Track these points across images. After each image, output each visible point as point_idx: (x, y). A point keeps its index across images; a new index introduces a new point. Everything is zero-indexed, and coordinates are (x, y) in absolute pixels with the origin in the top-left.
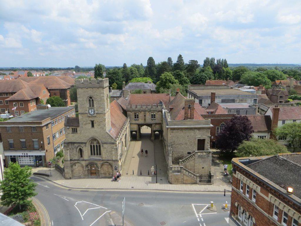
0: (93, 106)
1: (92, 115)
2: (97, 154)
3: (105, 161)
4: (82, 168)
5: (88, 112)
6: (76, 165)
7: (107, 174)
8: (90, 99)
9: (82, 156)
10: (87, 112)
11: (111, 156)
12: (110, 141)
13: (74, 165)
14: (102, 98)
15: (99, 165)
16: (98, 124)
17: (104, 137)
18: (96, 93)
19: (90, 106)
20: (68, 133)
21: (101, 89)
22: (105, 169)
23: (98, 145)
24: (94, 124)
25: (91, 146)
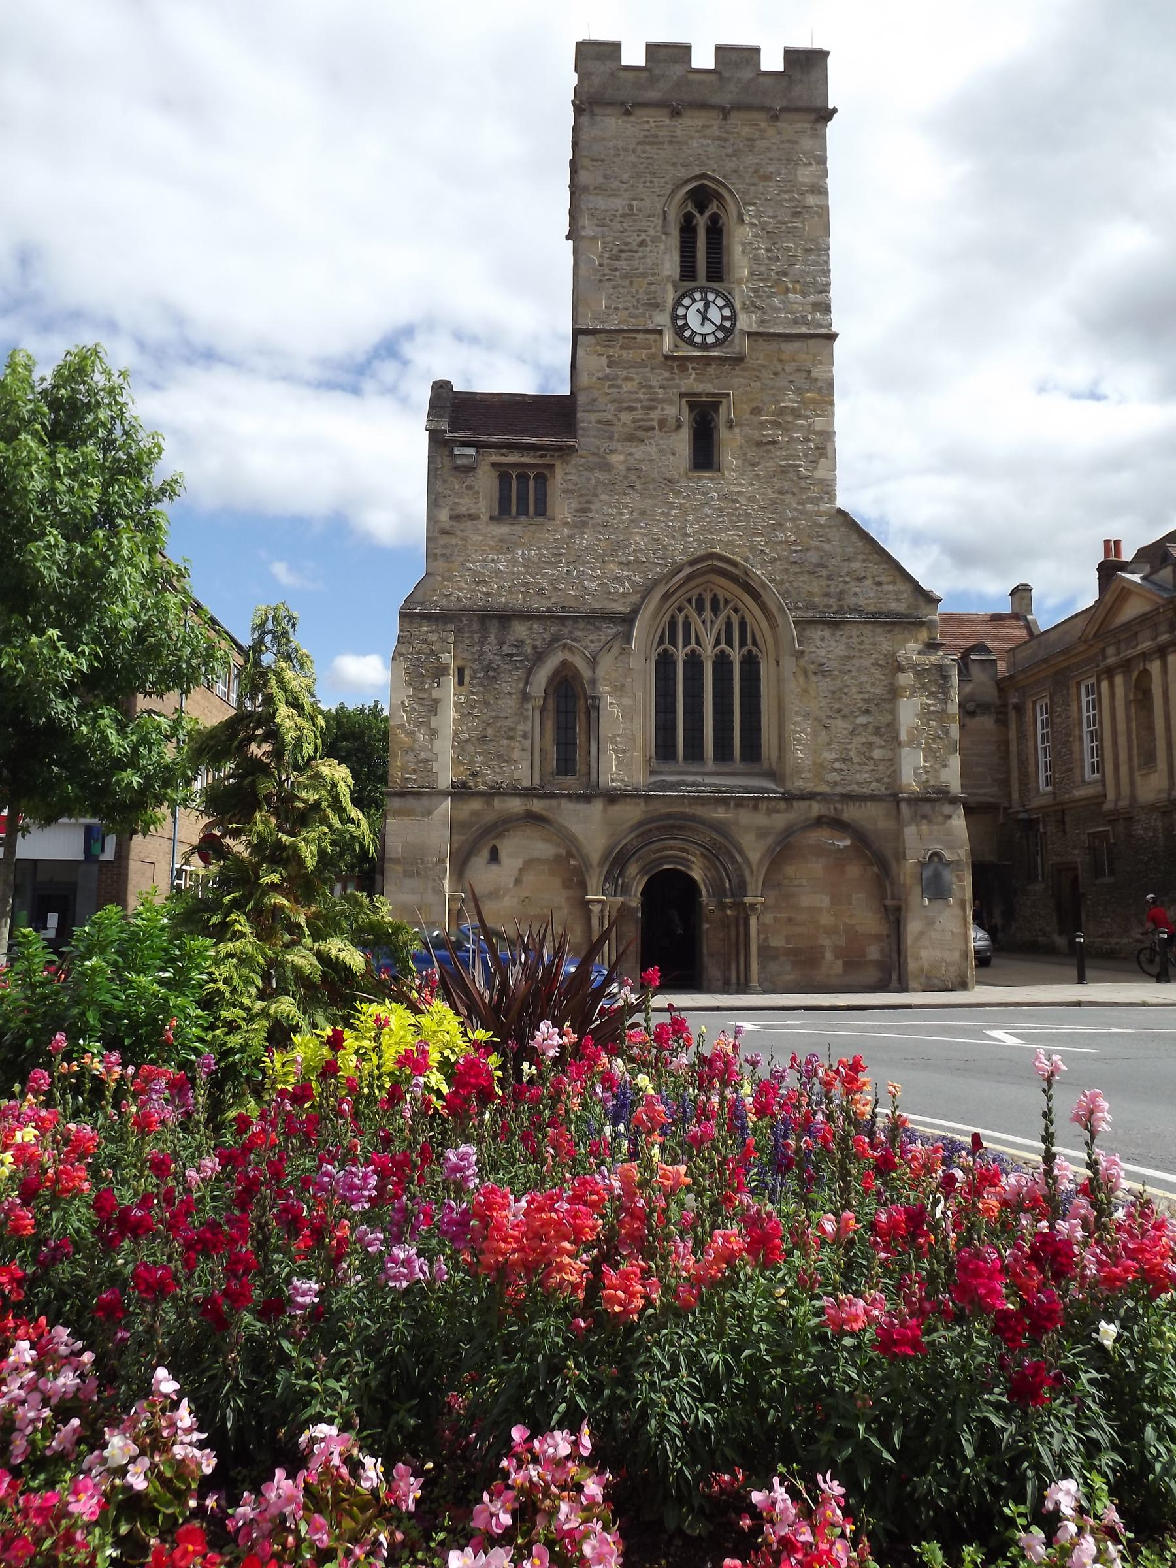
0: (717, 271)
1: (704, 346)
2: (723, 752)
3: (816, 809)
4: (566, 885)
5: (675, 317)
6: (503, 854)
7: (829, 955)
8: (690, 208)
9: (566, 765)
10: (662, 319)
11: (877, 754)
12: (865, 595)
13: (485, 853)
14: (811, 200)
15: (754, 851)
16: (756, 434)
17: (813, 557)
18: (750, 160)
19: (688, 271)
20: (456, 518)
21: (808, 126)
22: (806, 901)
23: (736, 656)
24: (724, 433)
25: (665, 664)
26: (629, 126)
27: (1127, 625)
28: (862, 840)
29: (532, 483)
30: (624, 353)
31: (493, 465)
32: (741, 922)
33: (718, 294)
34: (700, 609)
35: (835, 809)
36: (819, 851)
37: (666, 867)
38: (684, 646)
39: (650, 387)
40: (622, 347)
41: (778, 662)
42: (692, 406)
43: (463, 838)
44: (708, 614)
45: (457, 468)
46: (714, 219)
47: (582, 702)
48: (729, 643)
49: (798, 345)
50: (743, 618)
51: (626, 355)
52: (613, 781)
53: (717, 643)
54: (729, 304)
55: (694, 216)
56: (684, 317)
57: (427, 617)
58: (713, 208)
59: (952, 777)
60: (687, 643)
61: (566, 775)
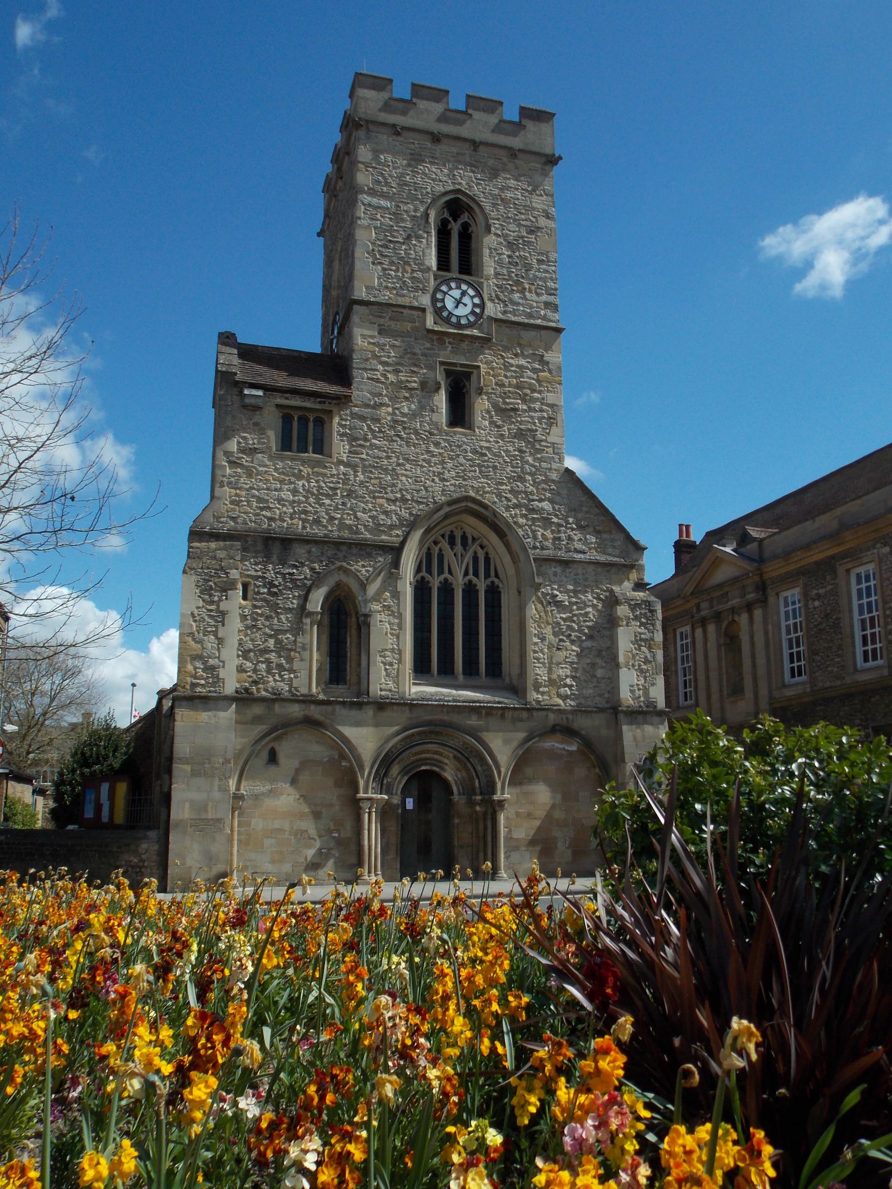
1: (458, 326)
2: (471, 668)
4: (338, 784)
5: (434, 300)
6: (281, 757)
8: (446, 215)
10: (425, 300)
11: (600, 673)
13: (265, 755)
19: (443, 263)
21: (538, 166)
23: (481, 586)
25: (421, 590)
26: (398, 144)
27: (720, 586)
28: (587, 744)
29: (311, 425)
30: (392, 324)
31: (278, 406)
32: (489, 817)
33: (470, 285)
34: (452, 543)
35: (567, 719)
36: (552, 755)
37: (423, 768)
38: (439, 575)
39: (415, 354)
40: (390, 319)
41: (519, 592)
42: (448, 373)
43: (245, 740)
44: (459, 548)
45: (245, 406)
46: (465, 226)
47: (354, 619)
48: (476, 574)
49: (532, 333)
50: (487, 554)
51: (392, 324)
52: (381, 690)
53: (466, 574)
54: (479, 294)
55: (449, 222)
56: (443, 300)
57: (215, 536)
58: (465, 217)
59: (658, 694)
60: (441, 571)
61: (338, 684)
